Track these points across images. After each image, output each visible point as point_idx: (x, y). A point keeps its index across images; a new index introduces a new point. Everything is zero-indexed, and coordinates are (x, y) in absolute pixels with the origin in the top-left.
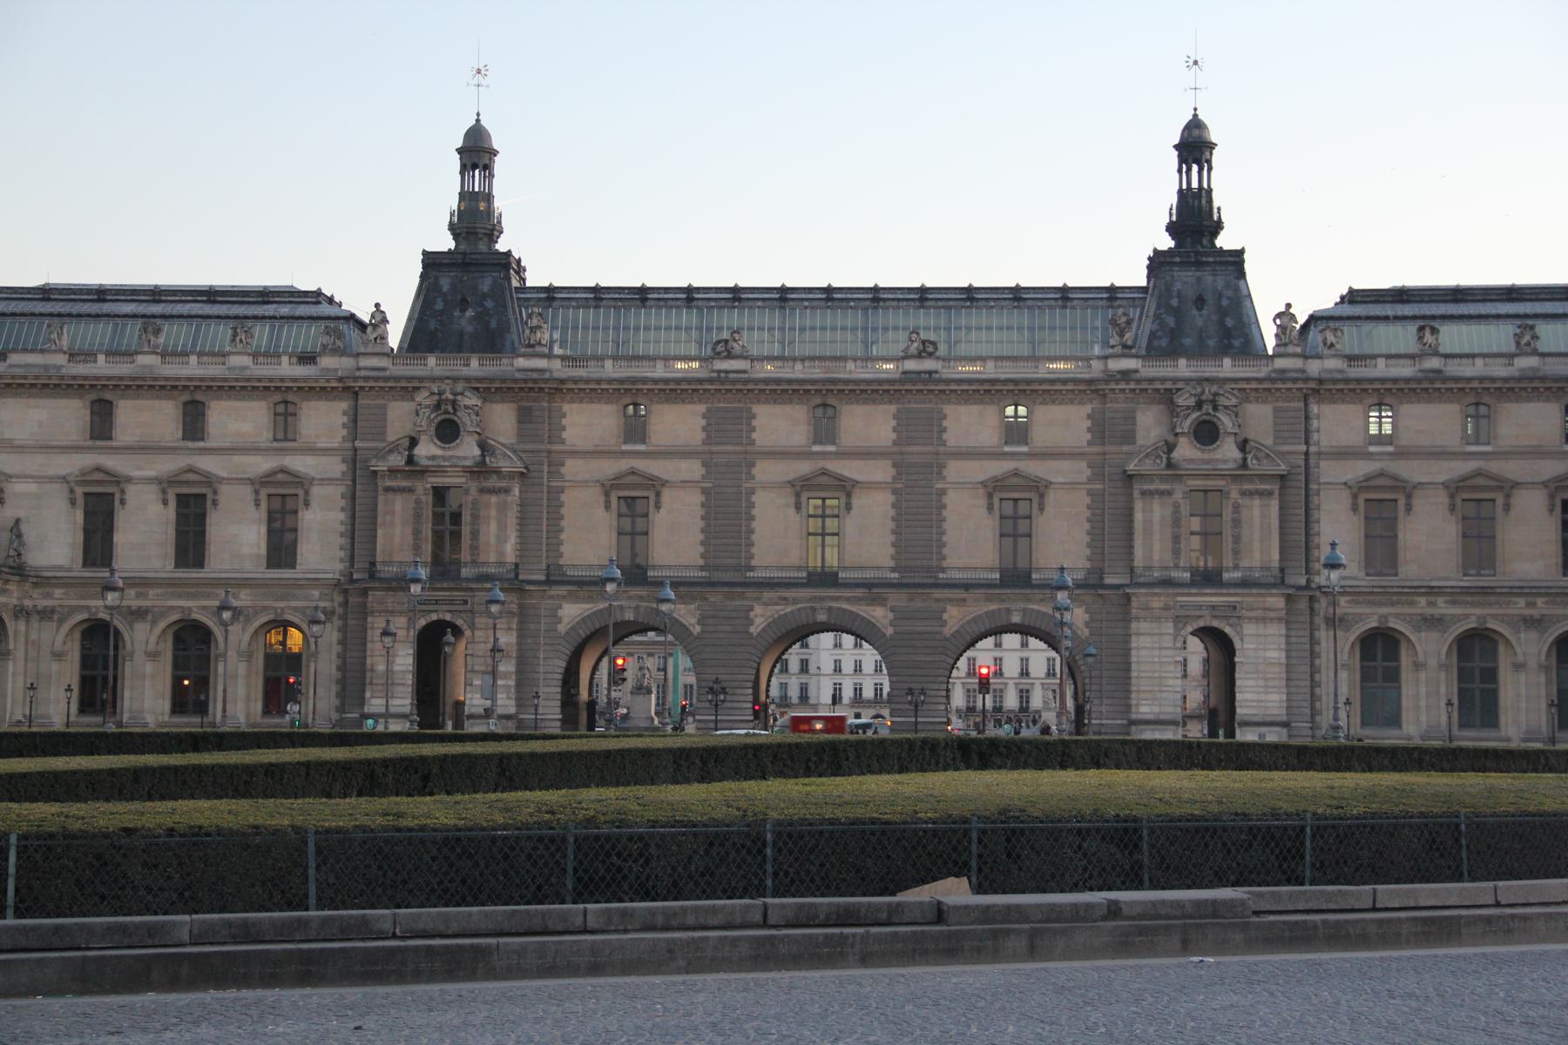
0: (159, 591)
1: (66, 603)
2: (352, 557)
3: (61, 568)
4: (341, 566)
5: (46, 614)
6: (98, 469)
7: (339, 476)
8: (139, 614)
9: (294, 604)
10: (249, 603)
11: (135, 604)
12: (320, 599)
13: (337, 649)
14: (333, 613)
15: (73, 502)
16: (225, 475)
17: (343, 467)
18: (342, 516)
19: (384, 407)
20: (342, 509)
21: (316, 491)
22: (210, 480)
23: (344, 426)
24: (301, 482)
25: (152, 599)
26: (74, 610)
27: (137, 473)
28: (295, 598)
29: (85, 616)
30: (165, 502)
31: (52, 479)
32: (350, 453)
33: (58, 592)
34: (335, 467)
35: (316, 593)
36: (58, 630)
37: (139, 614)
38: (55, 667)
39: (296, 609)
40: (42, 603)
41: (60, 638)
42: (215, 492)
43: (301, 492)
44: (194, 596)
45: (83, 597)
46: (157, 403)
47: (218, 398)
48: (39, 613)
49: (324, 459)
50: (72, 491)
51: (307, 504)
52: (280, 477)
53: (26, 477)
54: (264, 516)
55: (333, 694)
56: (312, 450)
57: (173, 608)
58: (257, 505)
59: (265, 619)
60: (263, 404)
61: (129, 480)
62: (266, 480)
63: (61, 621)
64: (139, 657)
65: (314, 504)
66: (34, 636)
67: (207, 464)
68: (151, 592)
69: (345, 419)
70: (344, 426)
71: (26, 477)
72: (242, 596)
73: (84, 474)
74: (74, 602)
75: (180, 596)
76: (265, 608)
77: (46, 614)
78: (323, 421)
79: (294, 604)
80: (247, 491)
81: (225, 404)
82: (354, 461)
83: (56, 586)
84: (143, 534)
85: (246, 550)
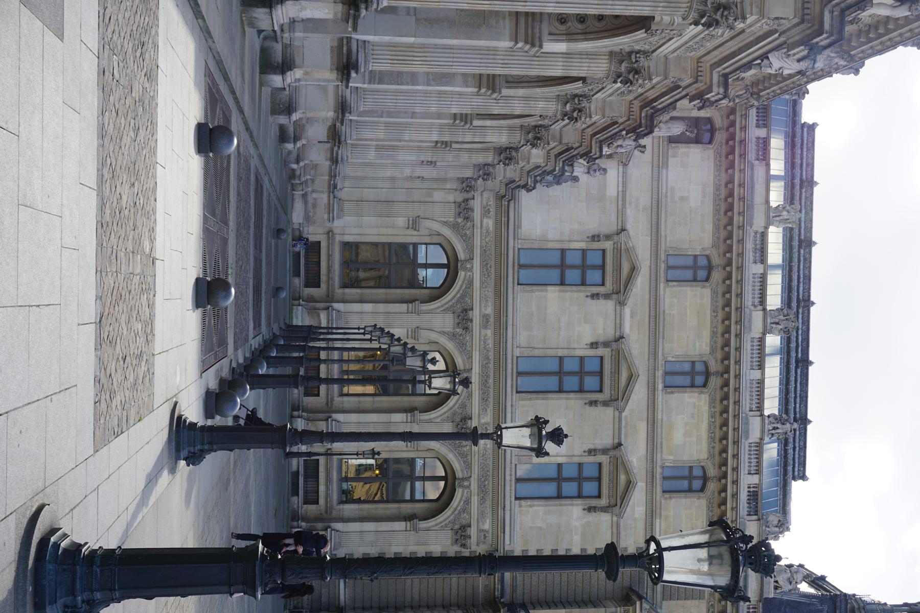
0: (490, 343)
1: (477, 233)
3: (518, 226)
5: (464, 209)
6: (633, 269)
8: (463, 318)
9: (475, 500)
11: (476, 315)
12: (480, 531)
13: (421, 552)
14: (464, 546)
15: (595, 238)
16: (624, 414)
20: (583, 550)
21: (605, 519)
22: (618, 399)
24: (617, 503)
25: (481, 335)
27: (627, 311)
28: (482, 501)
29: (461, 255)
30: (594, 345)
31: (621, 214)
33: (490, 223)
35: (487, 526)
36: (445, 223)
37: (463, 318)
38: (401, 221)
39: (468, 502)
40: (477, 205)
41: (436, 226)
42: (606, 404)
43: (604, 502)
45: (484, 252)
48: (466, 200)
50: (608, 237)
51: (590, 509)
53: (624, 184)
54: (577, 460)
56: (652, 514)
57: (470, 357)
58: (592, 452)
59: (457, 466)
61: (622, 304)
62: (619, 464)
63: (455, 227)
64: (413, 321)
65: (593, 517)
66: (438, 196)
68: (489, 332)
73: (627, 250)
74: (477, 242)
75: (484, 367)
76: (468, 466)
77: (464, 209)
79: (475, 500)
80: (605, 440)
83: (498, 223)
84: (561, 321)
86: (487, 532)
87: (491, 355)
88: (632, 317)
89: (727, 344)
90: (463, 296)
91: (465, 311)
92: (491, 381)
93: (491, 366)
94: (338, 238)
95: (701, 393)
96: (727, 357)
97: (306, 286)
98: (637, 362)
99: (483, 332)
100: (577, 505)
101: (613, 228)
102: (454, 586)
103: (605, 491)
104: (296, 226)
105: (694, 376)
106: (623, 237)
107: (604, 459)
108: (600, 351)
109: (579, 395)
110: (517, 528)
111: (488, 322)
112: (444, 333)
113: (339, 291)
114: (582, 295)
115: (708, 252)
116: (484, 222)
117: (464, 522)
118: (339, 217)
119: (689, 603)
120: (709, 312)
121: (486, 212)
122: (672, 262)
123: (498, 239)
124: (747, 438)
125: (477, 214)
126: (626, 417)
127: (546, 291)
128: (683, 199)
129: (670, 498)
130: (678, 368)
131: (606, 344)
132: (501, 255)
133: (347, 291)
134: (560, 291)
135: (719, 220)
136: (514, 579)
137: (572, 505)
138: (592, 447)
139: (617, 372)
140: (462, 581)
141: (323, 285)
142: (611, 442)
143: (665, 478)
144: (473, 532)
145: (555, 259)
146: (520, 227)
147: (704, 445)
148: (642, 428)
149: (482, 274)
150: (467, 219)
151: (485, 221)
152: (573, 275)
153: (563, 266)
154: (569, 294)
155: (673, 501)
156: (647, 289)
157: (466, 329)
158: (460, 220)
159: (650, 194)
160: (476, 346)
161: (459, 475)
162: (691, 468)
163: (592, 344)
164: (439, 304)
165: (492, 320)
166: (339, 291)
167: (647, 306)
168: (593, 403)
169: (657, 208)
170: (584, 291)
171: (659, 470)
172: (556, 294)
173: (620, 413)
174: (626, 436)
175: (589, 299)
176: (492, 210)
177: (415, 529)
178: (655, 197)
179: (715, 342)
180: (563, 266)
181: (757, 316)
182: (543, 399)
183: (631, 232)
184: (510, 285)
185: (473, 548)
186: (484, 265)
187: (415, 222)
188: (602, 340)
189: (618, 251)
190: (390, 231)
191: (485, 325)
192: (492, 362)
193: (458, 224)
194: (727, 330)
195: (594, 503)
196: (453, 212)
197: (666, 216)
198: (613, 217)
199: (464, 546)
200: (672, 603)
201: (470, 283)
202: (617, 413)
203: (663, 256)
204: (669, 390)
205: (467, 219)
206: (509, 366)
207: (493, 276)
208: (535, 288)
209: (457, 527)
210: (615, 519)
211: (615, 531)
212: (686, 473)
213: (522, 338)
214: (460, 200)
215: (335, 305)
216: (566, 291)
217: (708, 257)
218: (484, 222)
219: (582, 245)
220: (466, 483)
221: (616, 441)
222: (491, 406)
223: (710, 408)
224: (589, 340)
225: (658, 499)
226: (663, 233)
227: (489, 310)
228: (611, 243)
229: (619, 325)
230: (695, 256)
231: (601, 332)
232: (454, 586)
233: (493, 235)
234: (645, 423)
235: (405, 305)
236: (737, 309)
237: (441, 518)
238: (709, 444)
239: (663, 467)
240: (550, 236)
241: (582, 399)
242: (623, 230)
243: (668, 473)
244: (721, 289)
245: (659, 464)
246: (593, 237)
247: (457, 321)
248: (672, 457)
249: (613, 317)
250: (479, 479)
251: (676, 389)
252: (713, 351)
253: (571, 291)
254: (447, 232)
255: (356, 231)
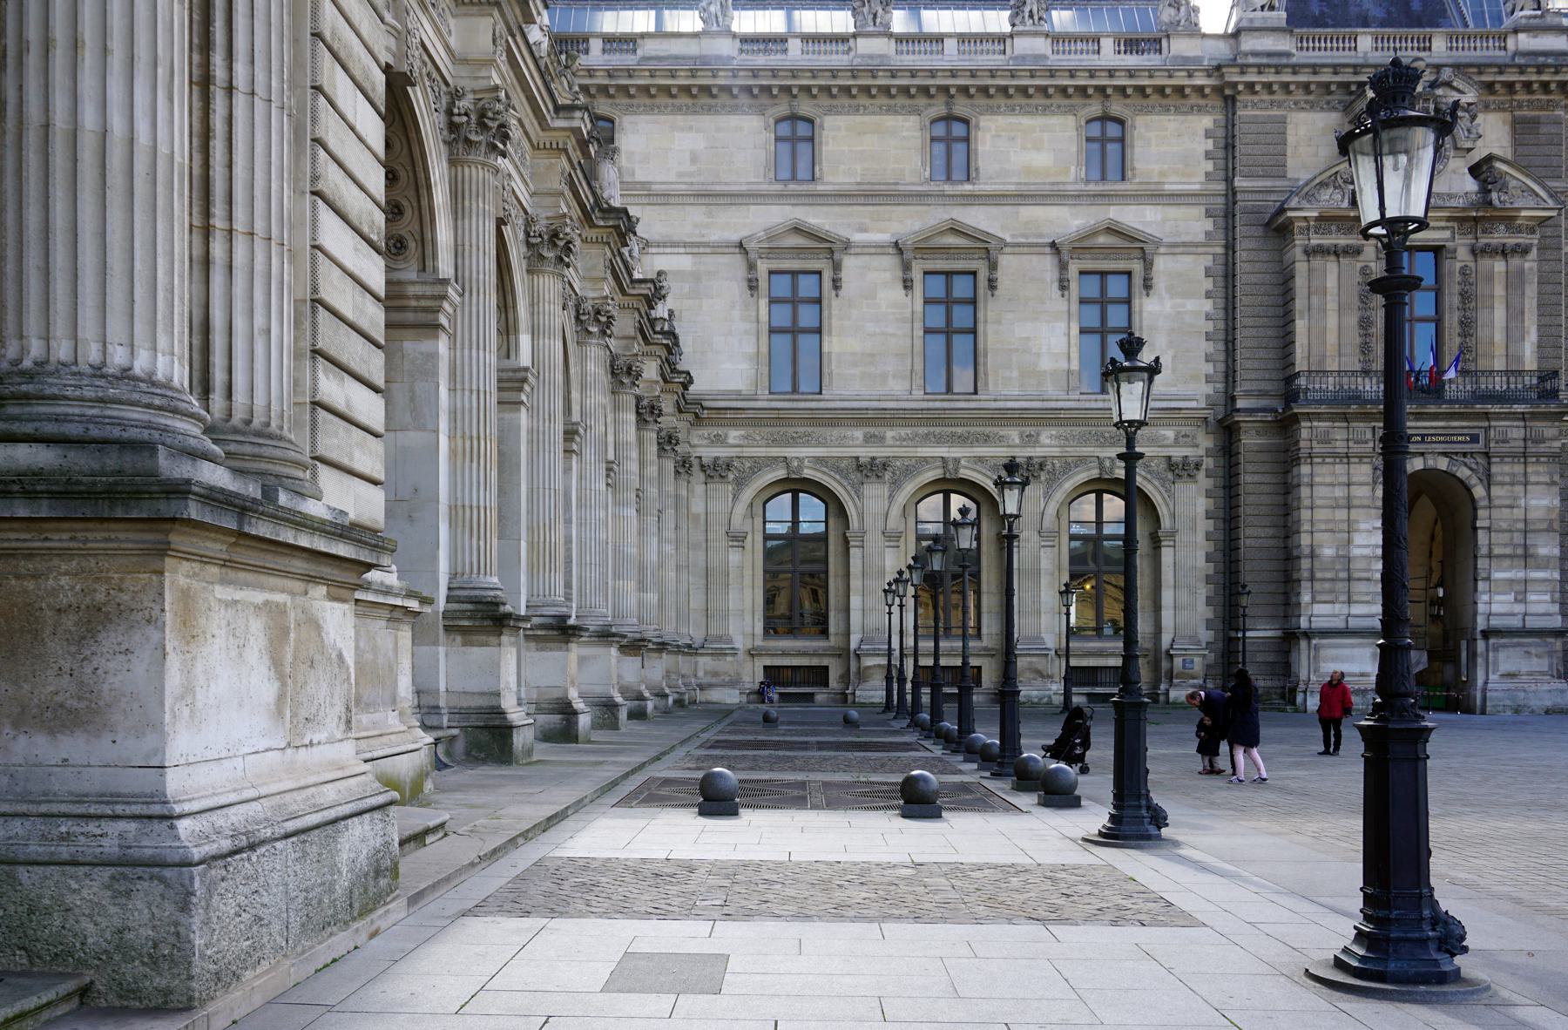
0: (903, 432)
1: (748, 452)
2: (1230, 376)
3: (738, 395)
4: (1208, 389)
5: (715, 471)
6: (797, 230)
7: (1201, 238)
8: (871, 470)
10: (1056, 451)
11: (865, 453)
15: (752, 285)
17: (1208, 225)
18: (1208, 306)
19: (1283, 121)
20: (1208, 295)
21: (1161, 264)
22: (986, 248)
23: (1208, 155)
24: (1139, 247)
25: (892, 445)
26: (759, 465)
27: (857, 237)
29: (781, 473)
30: (907, 285)
31: (717, 248)
32: (1221, 200)
33: (734, 435)
34: (1195, 224)
36: (735, 497)
37: (871, 470)
38: (734, 557)
40: (708, 453)
41: (740, 509)
42: (993, 266)
43: (1137, 267)
44: (963, 440)
45: (775, 442)
46: (889, 121)
47: (993, 111)
49: (1172, 212)
50: (751, 267)
51: (1148, 286)
52: (1102, 240)
53: (674, 245)
54: (1075, 306)
55: (1202, 599)
56: (1157, 196)
57: (925, 460)
58: (1063, 286)
59: (1082, 477)
60: (1070, 121)
61: (847, 246)
62: (1082, 246)
63: (740, 483)
64: (874, 539)
65: (1160, 282)
66: (698, 507)
67: (979, 218)
69: (1210, 144)
70: (1208, 155)
71: (674, 245)
72: (1044, 439)
73: (770, 239)
74: (761, 452)
75: (940, 440)
76: (1082, 460)
77: (715, 471)
78: (1174, 147)
80: (1046, 266)
81: (1001, 121)
82: (1229, 215)
83: (734, 423)
84: (872, 333)
85: (1046, 364)
86: (1178, 433)
87: (922, 430)
88: (866, 231)
89: (905, 90)
90: (838, 470)
91: (859, 467)
92: (959, 430)
93: (938, 430)
94: (759, 642)
95: (977, 127)
96: (925, 90)
97: (827, 685)
98: (933, 222)
99: (889, 442)
100: (1141, 305)
101: (738, 260)
102: (1256, 478)
103: (1122, 265)
104: (744, 698)
105: (952, 139)
106: (750, 246)
107: (1074, 268)
108: (917, 275)
109: (981, 305)
110: (1173, 390)
111: (874, 436)
112: (891, 497)
113: (834, 641)
114: (835, 303)
115: (772, 121)
116: (734, 442)
117: (1163, 466)
118: (730, 641)
119: (1291, 139)
120: (858, 118)
121: (719, 440)
122: (786, 174)
123: (756, 422)
124: (1045, 57)
125: (722, 452)
126: (1013, 236)
127: (830, 353)
128: (694, 159)
129: (1133, 169)
130: (940, 162)
131: (906, 267)
132: (778, 419)
133: (832, 630)
134: (830, 333)
135: (723, 107)
136: (1248, 394)
137: (1141, 312)
138: (1056, 285)
139: (945, 251)
140: (1250, 468)
141: (825, 662)
142: (1049, 258)
143: (1103, 178)
144: (1178, 453)
145: (784, 341)
146: (738, 393)
147: (1055, 121)
148: (1029, 212)
149: (807, 444)
150: (728, 467)
151: (731, 441)
152: (807, 316)
153: (794, 331)
154: (834, 322)
155: (1137, 165)
156: (825, 209)
157: (885, 466)
158: (731, 476)
159: (688, 208)
160: (911, 452)
161: (1095, 473)
162: (1088, 140)
163: (906, 287)
164: (850, 503)
165: (872, 430)
166: (834, 641)
167: (850, 209)
168: (992, 284)
169: (709, 197)
170: (830, 299)
171: (1092, 187)
172: (835, 339)
173: (1007, 245)
174: (1040, 236)
175: (841, 293)
176: (715, 431)
177: (1172, 534)
178: (692, 200)
179: (903, 107)
180: (794, 331)
181: (865, 46)
182: (986, 356)
183: (744, 233)
184: (822, 405)
185: (1201, 452)
186: (793, 441)
187: (735, 538)
188: (900, 274)
189: (772, 252)
190: (748, 573)
191: (880, 440)
192: (932, 429)
193: (736, 479)
194: (885, 90)
195: (1138, 281)
196: (719, 486)
197: (719, 183)
198: (722, 259)
199: (1198, 466)
200: (1290, 163)
201: (819, 460)
202: (1007, 250)
203: (779, 187)
204: (973, 174)
205: (728, 467)
206: (938, 405)
207: (810, 429)
208: (825, 370)
209: (1170, 476)
210: (1162, 250)
211: (1181, 250)
212: (1096, 146)
213: (897, 387)
214: (702, 476)
215: (853, 645)
216: (830, 325)
217: (777, 121)
218: (734, 442)
219: (764, 303)
220: (1107, 463)
221: (1048, 250)
222: (996, 429)
223: (1000, 114)
224: (899, 292)
225: (1135, 187)
226: (744, 188)
227: (859, 434)
228: (759, 262)
229: (877, 249)
230: (777, 139)
231: (888, 275)
232: (1256, 478)
233: (751, 430)
234: (1022, 209)
235: (852, 551)
236: (854, 77)
237: (1157, 499)
238: (1053, 113)
239: (1088, 181)
240: (751, 349)
241: (986, 301)
242: (741, 245)
243: (1096, 175)
244: (825, 101)
245: (1083, 187)
246: (751, 288)
247: (874, 479)
248: (1073, 169)
249: (867, 258)
250: (1102, 446)
251: (972, 164)
252: (916, 111)
253: (830, 318)
254: (748, 494)
255: (748, 618)
